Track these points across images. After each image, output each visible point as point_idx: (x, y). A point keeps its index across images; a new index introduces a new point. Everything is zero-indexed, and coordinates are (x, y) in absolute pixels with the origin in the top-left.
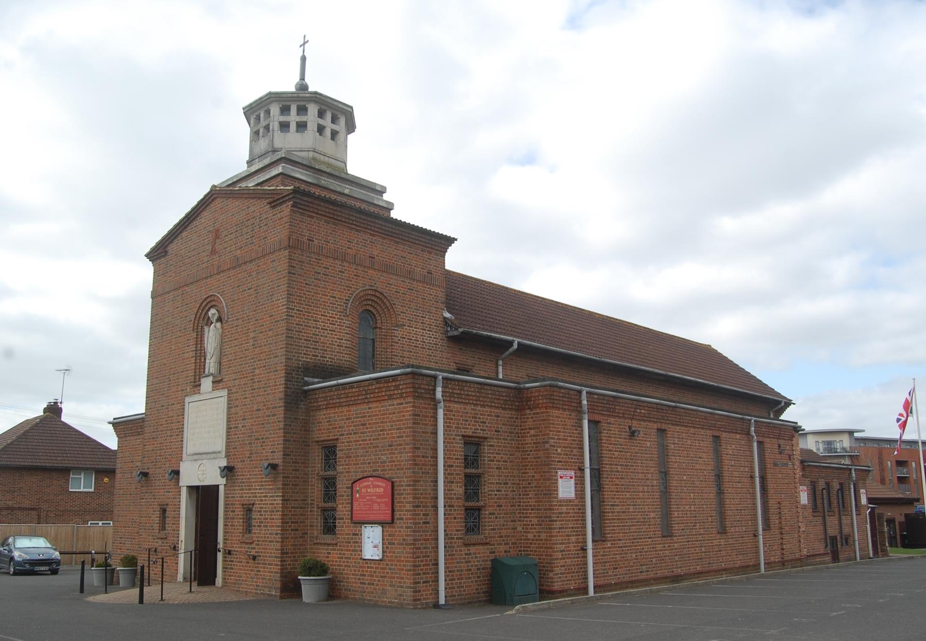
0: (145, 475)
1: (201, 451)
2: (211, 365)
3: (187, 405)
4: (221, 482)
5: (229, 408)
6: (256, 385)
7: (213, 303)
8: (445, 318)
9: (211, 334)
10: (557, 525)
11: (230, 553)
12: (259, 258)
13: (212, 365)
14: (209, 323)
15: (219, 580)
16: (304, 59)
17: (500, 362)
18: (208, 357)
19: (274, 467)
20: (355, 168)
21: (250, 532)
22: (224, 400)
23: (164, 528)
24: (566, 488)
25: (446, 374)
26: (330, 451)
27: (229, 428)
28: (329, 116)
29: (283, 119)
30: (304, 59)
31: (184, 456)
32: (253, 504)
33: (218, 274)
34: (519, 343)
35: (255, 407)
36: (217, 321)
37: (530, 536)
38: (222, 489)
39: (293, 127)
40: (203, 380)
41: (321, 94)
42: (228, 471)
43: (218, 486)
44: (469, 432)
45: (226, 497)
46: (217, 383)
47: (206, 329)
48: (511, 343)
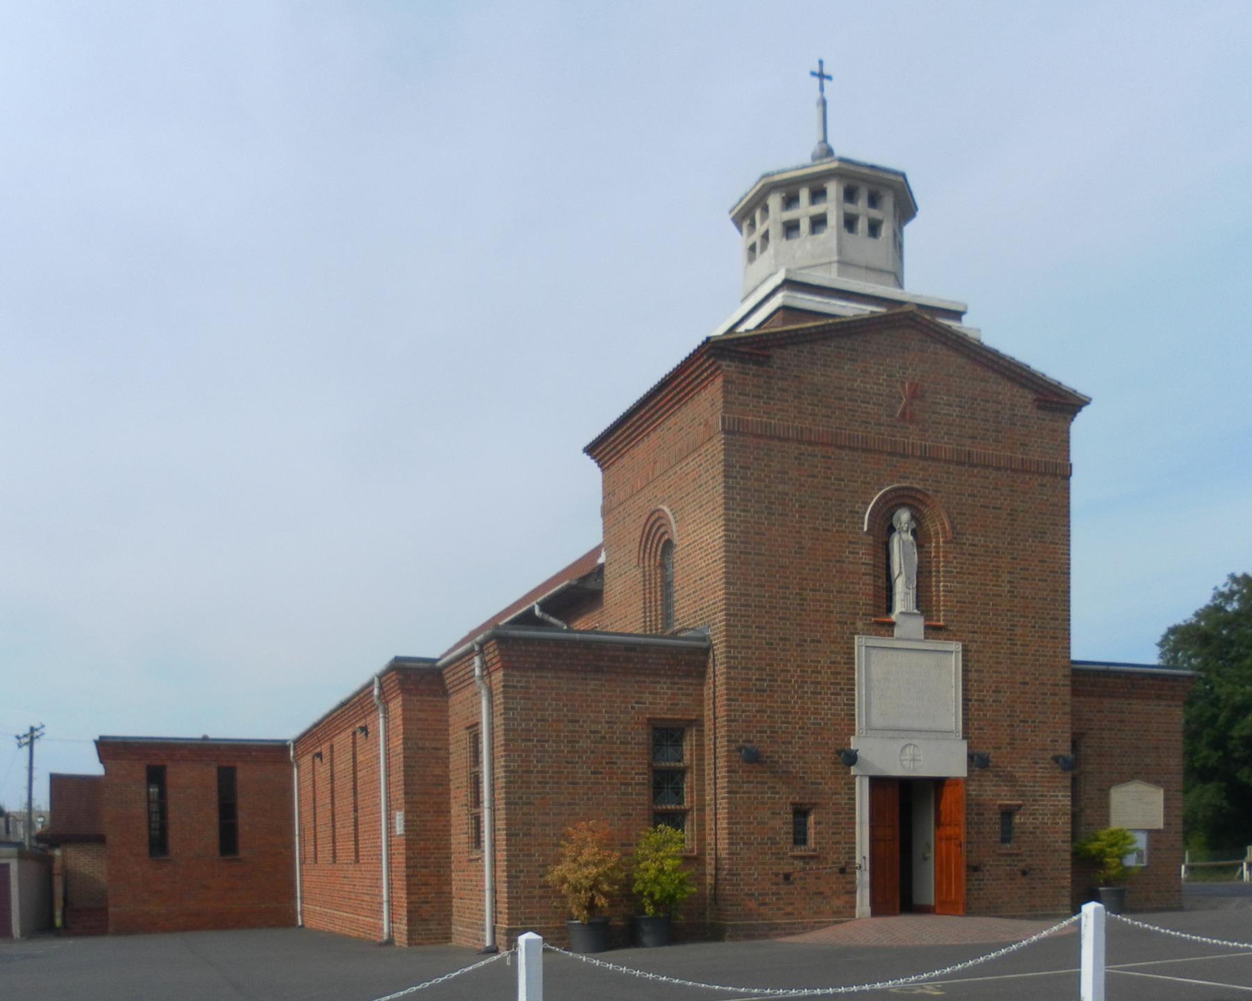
1: (903, 724)
5: (966, 670)
7: (909, 501)
12: (1014, 471)
27: (966, 700)
32: (1020, 806)
35: (1019, 678)
42: (977, 761)
46: (933, 631)
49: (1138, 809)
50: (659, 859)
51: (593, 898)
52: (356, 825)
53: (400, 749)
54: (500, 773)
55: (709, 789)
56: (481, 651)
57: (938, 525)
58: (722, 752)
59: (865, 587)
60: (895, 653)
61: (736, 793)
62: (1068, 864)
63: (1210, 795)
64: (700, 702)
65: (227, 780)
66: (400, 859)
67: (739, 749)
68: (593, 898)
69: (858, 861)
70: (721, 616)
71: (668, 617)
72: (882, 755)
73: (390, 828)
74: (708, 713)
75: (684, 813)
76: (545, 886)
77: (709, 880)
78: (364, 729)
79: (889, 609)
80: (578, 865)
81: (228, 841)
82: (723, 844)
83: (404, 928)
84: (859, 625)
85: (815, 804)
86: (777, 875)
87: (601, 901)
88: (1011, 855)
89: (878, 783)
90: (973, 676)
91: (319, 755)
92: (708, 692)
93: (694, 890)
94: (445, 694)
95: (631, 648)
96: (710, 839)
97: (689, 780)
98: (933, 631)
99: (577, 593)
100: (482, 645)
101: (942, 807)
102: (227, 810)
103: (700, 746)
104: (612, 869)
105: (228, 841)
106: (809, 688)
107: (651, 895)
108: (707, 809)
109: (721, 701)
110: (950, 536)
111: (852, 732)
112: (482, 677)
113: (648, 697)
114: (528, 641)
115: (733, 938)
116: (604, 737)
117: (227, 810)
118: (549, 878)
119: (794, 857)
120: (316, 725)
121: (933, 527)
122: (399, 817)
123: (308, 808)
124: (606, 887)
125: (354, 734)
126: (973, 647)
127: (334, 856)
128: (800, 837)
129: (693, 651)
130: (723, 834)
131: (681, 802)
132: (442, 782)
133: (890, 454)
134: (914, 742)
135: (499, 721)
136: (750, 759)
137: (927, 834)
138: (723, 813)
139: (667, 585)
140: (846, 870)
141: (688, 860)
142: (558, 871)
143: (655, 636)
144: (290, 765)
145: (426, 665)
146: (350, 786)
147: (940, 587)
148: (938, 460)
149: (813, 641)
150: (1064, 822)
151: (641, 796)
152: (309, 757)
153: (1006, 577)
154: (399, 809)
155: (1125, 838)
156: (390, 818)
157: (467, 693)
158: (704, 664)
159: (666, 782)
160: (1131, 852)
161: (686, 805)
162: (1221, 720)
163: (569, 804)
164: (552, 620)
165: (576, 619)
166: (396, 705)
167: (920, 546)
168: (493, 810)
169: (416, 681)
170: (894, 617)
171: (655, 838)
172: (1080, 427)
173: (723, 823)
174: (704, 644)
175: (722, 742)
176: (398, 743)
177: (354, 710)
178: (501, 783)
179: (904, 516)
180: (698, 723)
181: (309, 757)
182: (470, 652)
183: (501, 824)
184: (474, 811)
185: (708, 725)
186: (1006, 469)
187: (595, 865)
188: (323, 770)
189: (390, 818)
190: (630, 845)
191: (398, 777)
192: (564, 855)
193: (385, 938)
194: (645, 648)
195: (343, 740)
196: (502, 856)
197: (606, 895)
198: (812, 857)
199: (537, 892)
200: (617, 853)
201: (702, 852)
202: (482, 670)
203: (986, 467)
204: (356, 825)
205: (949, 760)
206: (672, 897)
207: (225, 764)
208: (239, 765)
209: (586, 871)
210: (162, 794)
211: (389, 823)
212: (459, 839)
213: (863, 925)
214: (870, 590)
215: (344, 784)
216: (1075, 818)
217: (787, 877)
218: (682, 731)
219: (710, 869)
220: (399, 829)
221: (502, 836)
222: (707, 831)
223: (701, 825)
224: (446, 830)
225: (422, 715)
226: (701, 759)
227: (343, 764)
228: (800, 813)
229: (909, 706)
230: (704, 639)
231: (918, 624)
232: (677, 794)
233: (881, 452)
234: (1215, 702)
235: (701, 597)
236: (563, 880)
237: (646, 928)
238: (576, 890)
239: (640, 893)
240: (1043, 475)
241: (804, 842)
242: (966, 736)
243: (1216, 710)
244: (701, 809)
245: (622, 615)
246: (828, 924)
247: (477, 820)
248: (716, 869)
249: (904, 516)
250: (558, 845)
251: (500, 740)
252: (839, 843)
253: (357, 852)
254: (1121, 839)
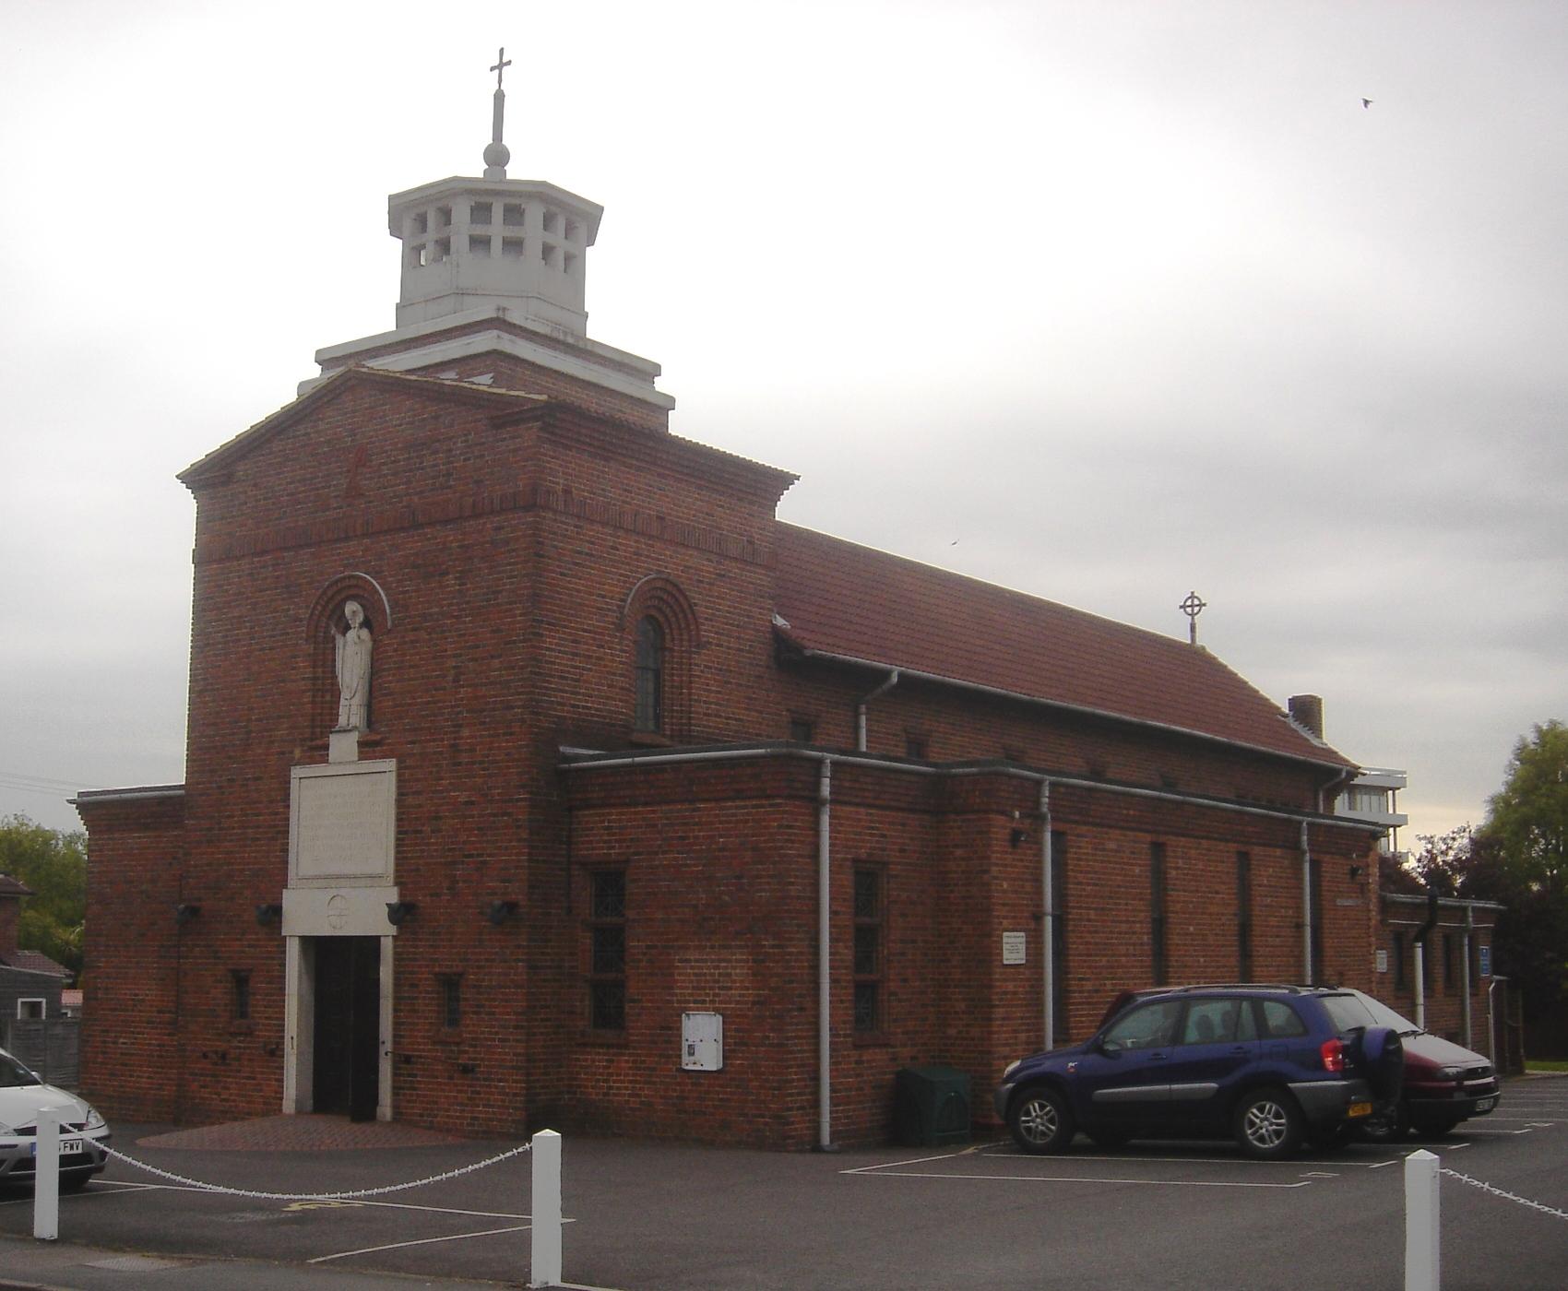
0: (194, 911)
2: (351, 710)
3: (294, 784)
4: (392, 930)
6: (464, 758)
7: (353, 591)
8: (774, 627)
9: (350, 649)
10: (999, 1012)
11: (408, 1060)
13: (354, 709)
14: (348, 628)
15: (385, 1108)
16: (499, 98)
17: (863, 708)
18: (345, 694)
19: (511, 907)
20: (604, 327)
21: (453, 1022)
22: (393, 777)
23: (243, 1015)
24: (1013, 948)
25: (837, 756)
26: (610, 880)
28: (561, 224)
29: (479, 230)
30: (499, 98)
31: (291, 883)
33: (365, 535)
34: (901, 675)
36: (362, 625)
37: (952, 1032)
38: (387, 948)
39: (497, 245)
40: (333, 738)
41: (553, 187)
43: (378, 938)
44: (863, 853)
45: (398, 957)
46: (369, 748)
47: (339, 640)
48: (887, 674)
84: (297, 753)
98: (369, 748)
242: (399, 882)
249: (351, 608)
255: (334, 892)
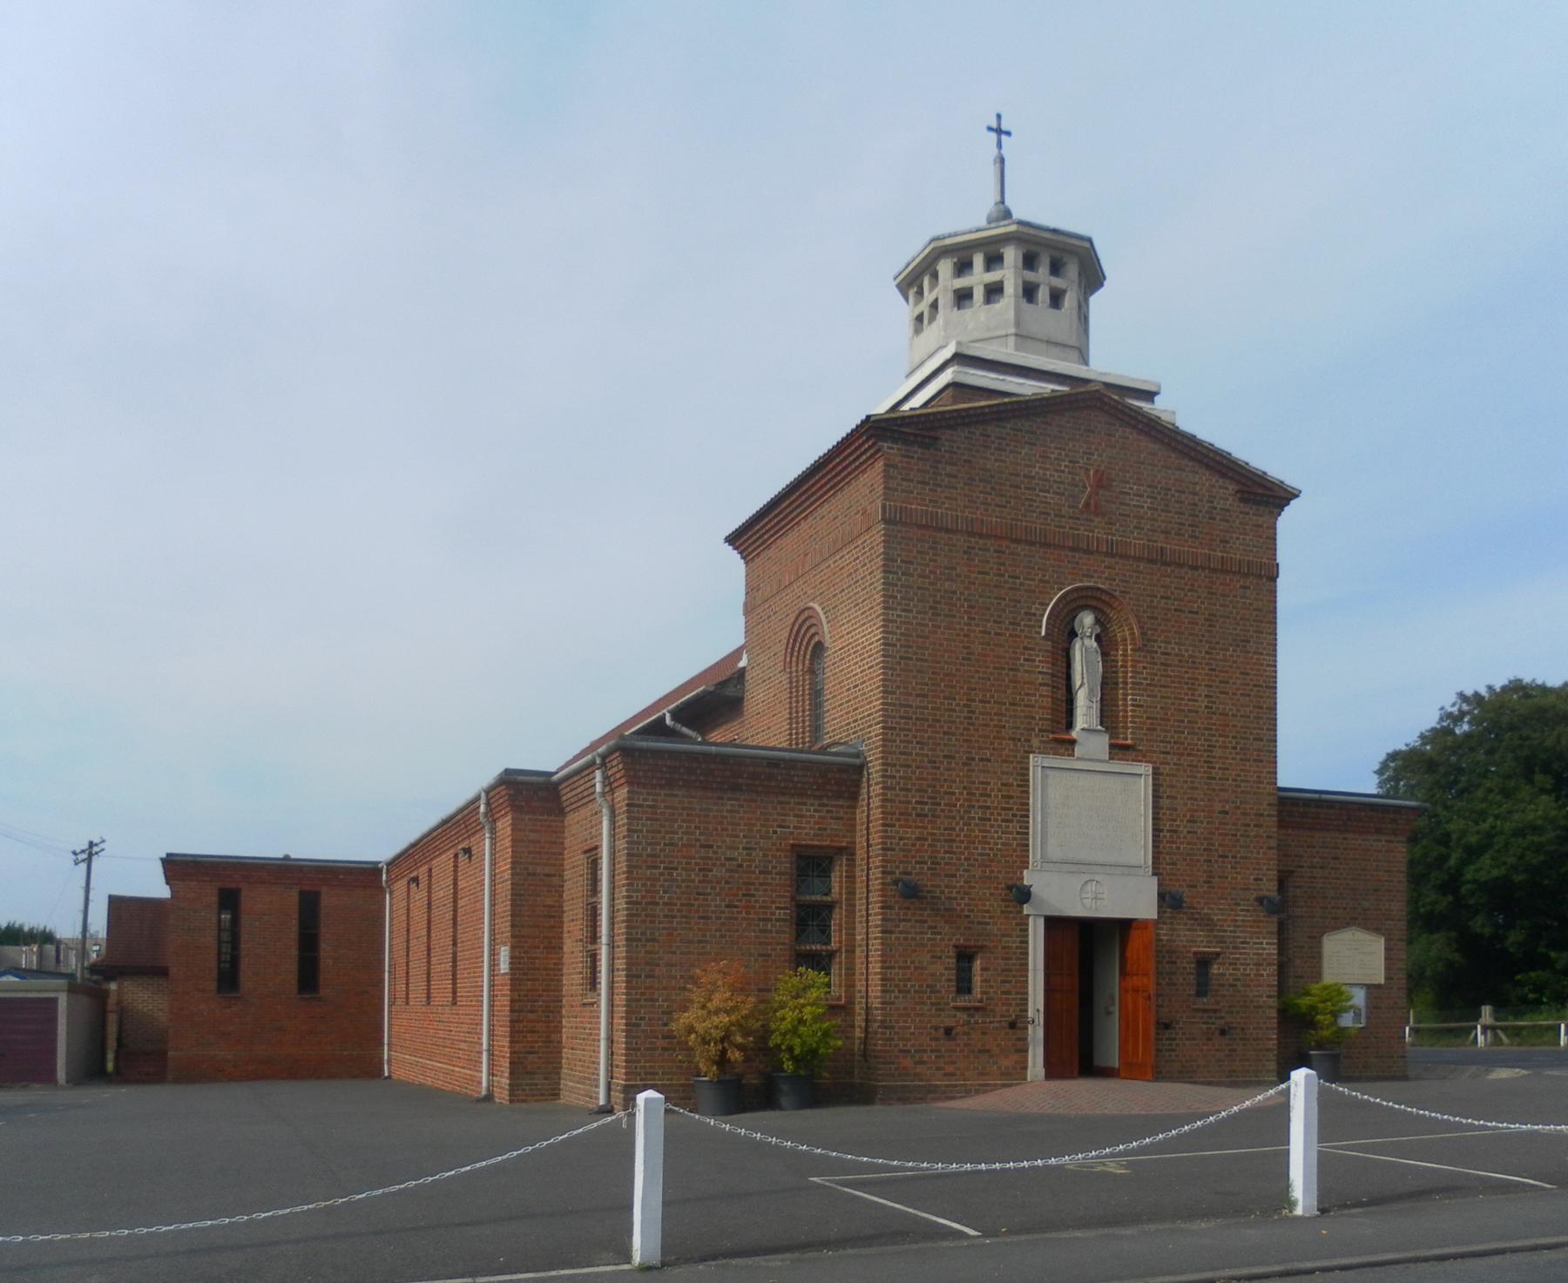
7: (1094, 603)
12: (1214, 570)
32: (1218, 954)
35: (1218, 807)
42: (1168, 900)
46: (1119, 750)
49: (1355, 961)
50: (799, 1004)
51: (724, 1052)
52: (454, 961)
53: (507, 875)
54: (621, 904)
55: (860, 928)
56: (603, 764)
57: (1126, 632)
58: (875, 884)
59: (1042, 699)
60: (1077, 775)
61: (891, 932)
62: (1274, 1023)
63: (1438, 948)
64: (852, 827)
65: (309, 907)
66: (504, 1002)
67: (896, 882)
68: (724, 1052)
69: (1030, 1014)
70: (878, 729)
71: (817, 730)
72: (1060, 891)
73: (494, 964)
74: (860, 841)
75: (831, 955)
76: (669, 1036)
77: (858, 1033)
78: (468, 851)
79: (1070, 725)
80: (707, 1013)
81: (308, 977)
82: (876, 990)
83: (505, 1081)
84: (1035, 742)
85: (982, 947)
86: (936, 1029)
87: (735, 1055)
88: (1205, 1011)
89: (1054, 924)
90: (1165, 802)
91: (416, 880)
92: (860, 816)
93: (840, 1043)
94: (561, 812)
95: (774, 763)
96: (860, 986)
97: (838, 917)
98: (1119, 750)
99: (713, 700)
100: (604, 757)
101: (1128, 954)
102: (308, 942)
103: (851, 878)
104: (745, 1017)
105: (308, 977)
106: (976, 814)
107: (790, 1049)
108: (858, 950)
109: (876, 826)
110: (1139, 643)
111: (1025, 864)
112: (603, 794)
113: (792, 821)
114: (656, 753)
115: (883, 1101)
116: (740, 866)
117: (308, 942)
118: (673, 1026)
119: (957, 1008)
120: (413, 846)
121: (1121, 633)
122: (504, 953)
123: (400, 941)
124: (739, 1039)
125: (456, 856)
126: (1165, 769)
127: (428, 997)
128: (964, 986)
129: (843, 768)
130: (875, 980)
131: (828, 943)
132: (555, 915)
133: (1073, 549)
134: (1097, 878)
135: (621, 844)
136: (908, 893)
137: (1111, 986)
138: (875, 956)
139: (816, 694)
140: (1017, 1025)
141: (834, 1009)
142: (685, 1018)
143: (802, 751)
144: (381, 890)
145: (541, 779)
146: (449, 915)
147: (1128, 700)
148: (1126, 557)
149: (981, 760)
150: (1269, 974)
151: (784, 935)
152: (404, 882)
153: (1203, 691)
154: (505, 944)
155: (1340, 993)
156: (494, 954)
157: (584, 812)
158: (857, 784)
159: (811, 918)
160: (1346, 1010)
161: (834, 945)
162: (1452, 862)
163: (700, 942)
164: (685, 730)
165: (712, 729)
166: (505, 824)
167: (1104, 654)
168: (612, 945)
169: (528, 798)
170: (1074, 734)
171: (795, 980)
172: (1289, 523)
173: (876, 968)
174: (857, 761)
175: (876, 873)
176: (505, 867)
177: (455, 831)
178: (621, 916)
179: (1087, 619)
180: (849, 851)
181: (404, 882)
182: (591, 765)
183: (620, 964)
184: (590, 947)
185: (860, 854)
186: (1204, 569)
187: (727, 1012)
188: (419, 896)
189: (494, 954)
190: (769, 990)
191: (505, 907)
192: (692, 1001)
193: (484, 1092)
194: (791, 764)
195: (443, 863)
196: (620, 999)
197: (741, 1048)
198: (977, 1009)
199: (660, 1043)
200: (752, 999)
201: (851, 1000)
202: (604, 786)
203: (1180, 565)
204: (454, 961)
205: (1134, 898)
206: (814, 1052)
207: (307, 888)
208: (324, 890)
209: (716, 1020)
210: (235, 921)
211: (493, 961)
212: (572, 979)
213: (1036, 1088)
214: (1047, 702)
215: (443, 914)
216: (1282, 969)
217: (948, 1031)
218: (831, 860)
219: (859, 1021)
220: (504, 967)
221: (621, 977)
222: (857, 976)
223: (850, 970)
224: (558, 968)
225: (533, 836)
226: (851, 893)
227: (442, 892)
228: (965, 957)
229: (1091, 838)
230: (857, 755)
231: (1101, 743)
232: (823, 932)
233: (1063, 547)
234: (1445, 840)
235: (855, 710)
236: (691, 1030)
237: (785, 1088)
238: (705, 1042)
239: (778, 1046)
240: (1247, 575)
241: (969, 991)
243: (1443, 850)
244: (851, 951)
245: (765, 726)
246: (995, 1087)
247: (594, 957)
248: (867, 1021)
249: (1087, 619)
250: (685, 989)
251: (622, 866)
252: (1008, 993)
253: (454, 992)
254: (1336, 994)
255: (1087, 877)
